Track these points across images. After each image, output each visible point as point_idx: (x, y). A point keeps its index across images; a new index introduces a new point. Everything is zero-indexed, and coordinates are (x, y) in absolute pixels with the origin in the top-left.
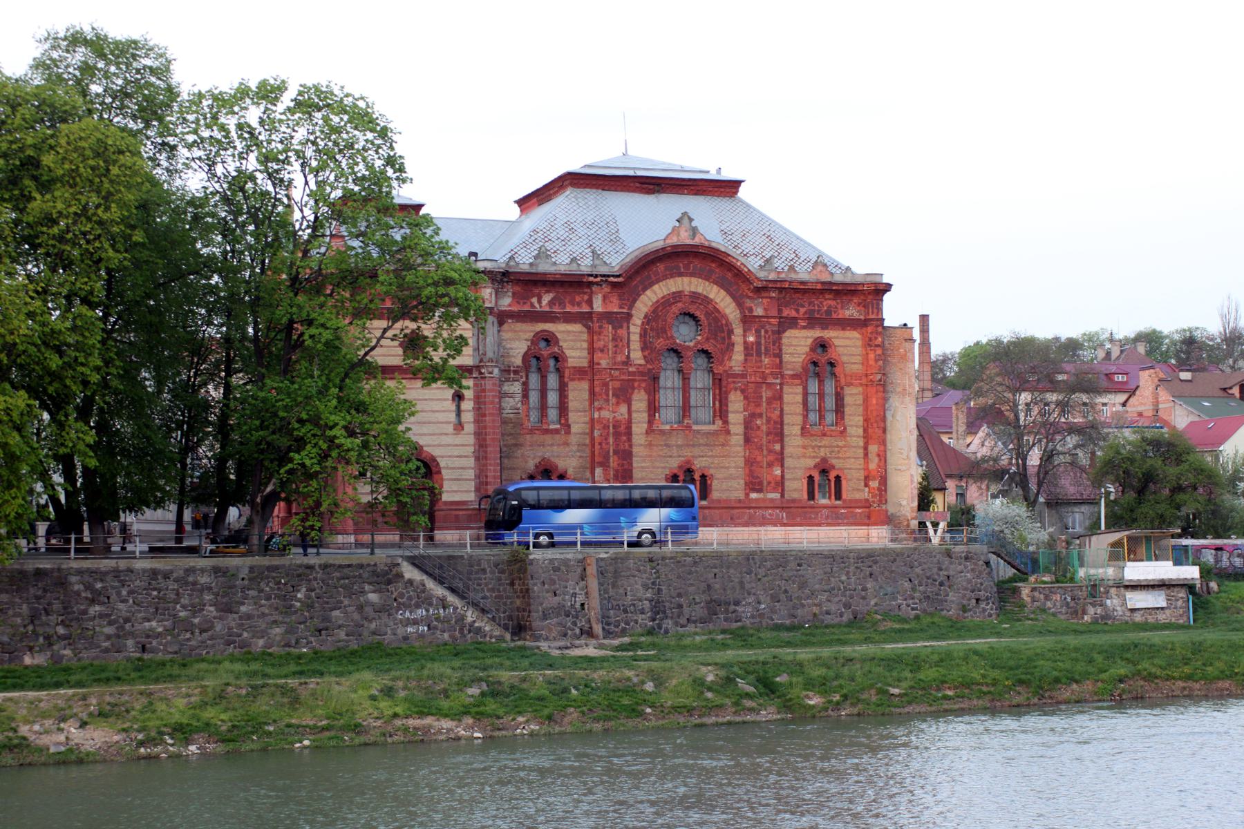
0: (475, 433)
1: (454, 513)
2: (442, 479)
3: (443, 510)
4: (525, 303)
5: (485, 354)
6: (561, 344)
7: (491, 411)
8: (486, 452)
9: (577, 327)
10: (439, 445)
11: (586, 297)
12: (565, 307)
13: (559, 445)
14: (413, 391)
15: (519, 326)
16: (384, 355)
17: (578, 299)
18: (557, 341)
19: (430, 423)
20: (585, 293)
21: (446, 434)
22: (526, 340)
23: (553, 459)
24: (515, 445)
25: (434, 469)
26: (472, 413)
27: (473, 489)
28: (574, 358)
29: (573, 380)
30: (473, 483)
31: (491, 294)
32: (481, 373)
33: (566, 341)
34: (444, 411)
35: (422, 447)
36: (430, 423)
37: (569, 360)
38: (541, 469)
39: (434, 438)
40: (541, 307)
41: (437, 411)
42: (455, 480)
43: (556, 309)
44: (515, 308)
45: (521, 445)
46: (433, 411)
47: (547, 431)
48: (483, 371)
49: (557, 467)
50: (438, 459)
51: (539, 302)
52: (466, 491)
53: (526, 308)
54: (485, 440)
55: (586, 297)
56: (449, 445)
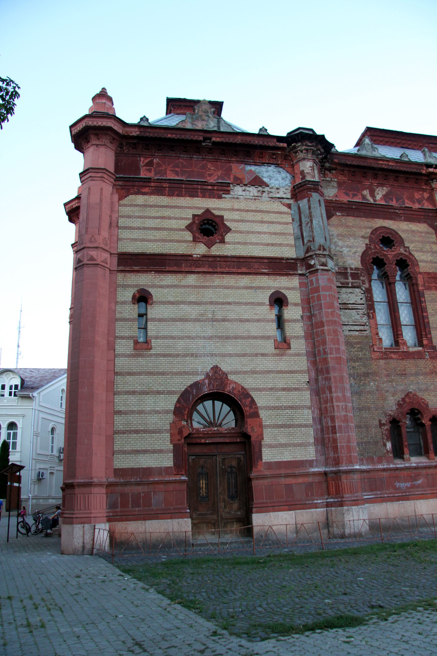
0: (308, 354)
1: (283, 481)
2: (261, 426)
3: (264, 477)
4: (354, 195)
5: (313, 240)
6: (407, 244)
7: (330, 318)
8: (328, 379)
9: (422, 227)
10: (254, 372)
11: (426, 195)
12: (404, 203)
13: (425, 374)
14: (210, 291)
15: (351, 221)
16: (164, 241)
17: (417, 196)
18: (402, 241)
19: (236, 338)
20: (424, 190)
21: (263, 355)
22: (363, 237)
23: (420, 394)
24: (367, 375)
25: (246, 409)
26: (301, 324)
27: (312, 440)
28: (426, 262)
29: (429, 288)
30: (311, 431)
31: (312, 167)
32: (309, 266)
33: (412, 242)
34: (258, 321)
35: (225, 375)
36: (236, 338)
37: (421, 264)
38: (406, 409)
39: (244, 360)
40: (375, 201)
41: (247, 320)
42: (282, 426)
43: (394, 203)
44: (345, 199)
45: (375, 374)
46: (241, 321)
47: (407, 355)
48: (312, 262)
49: (427, 405)
50: (253, 394)
51: (373, 195)
52: (300, 445)
53: (357, 199)
54: (325, 361)
55: (426, 195)
56: (269, 372)
